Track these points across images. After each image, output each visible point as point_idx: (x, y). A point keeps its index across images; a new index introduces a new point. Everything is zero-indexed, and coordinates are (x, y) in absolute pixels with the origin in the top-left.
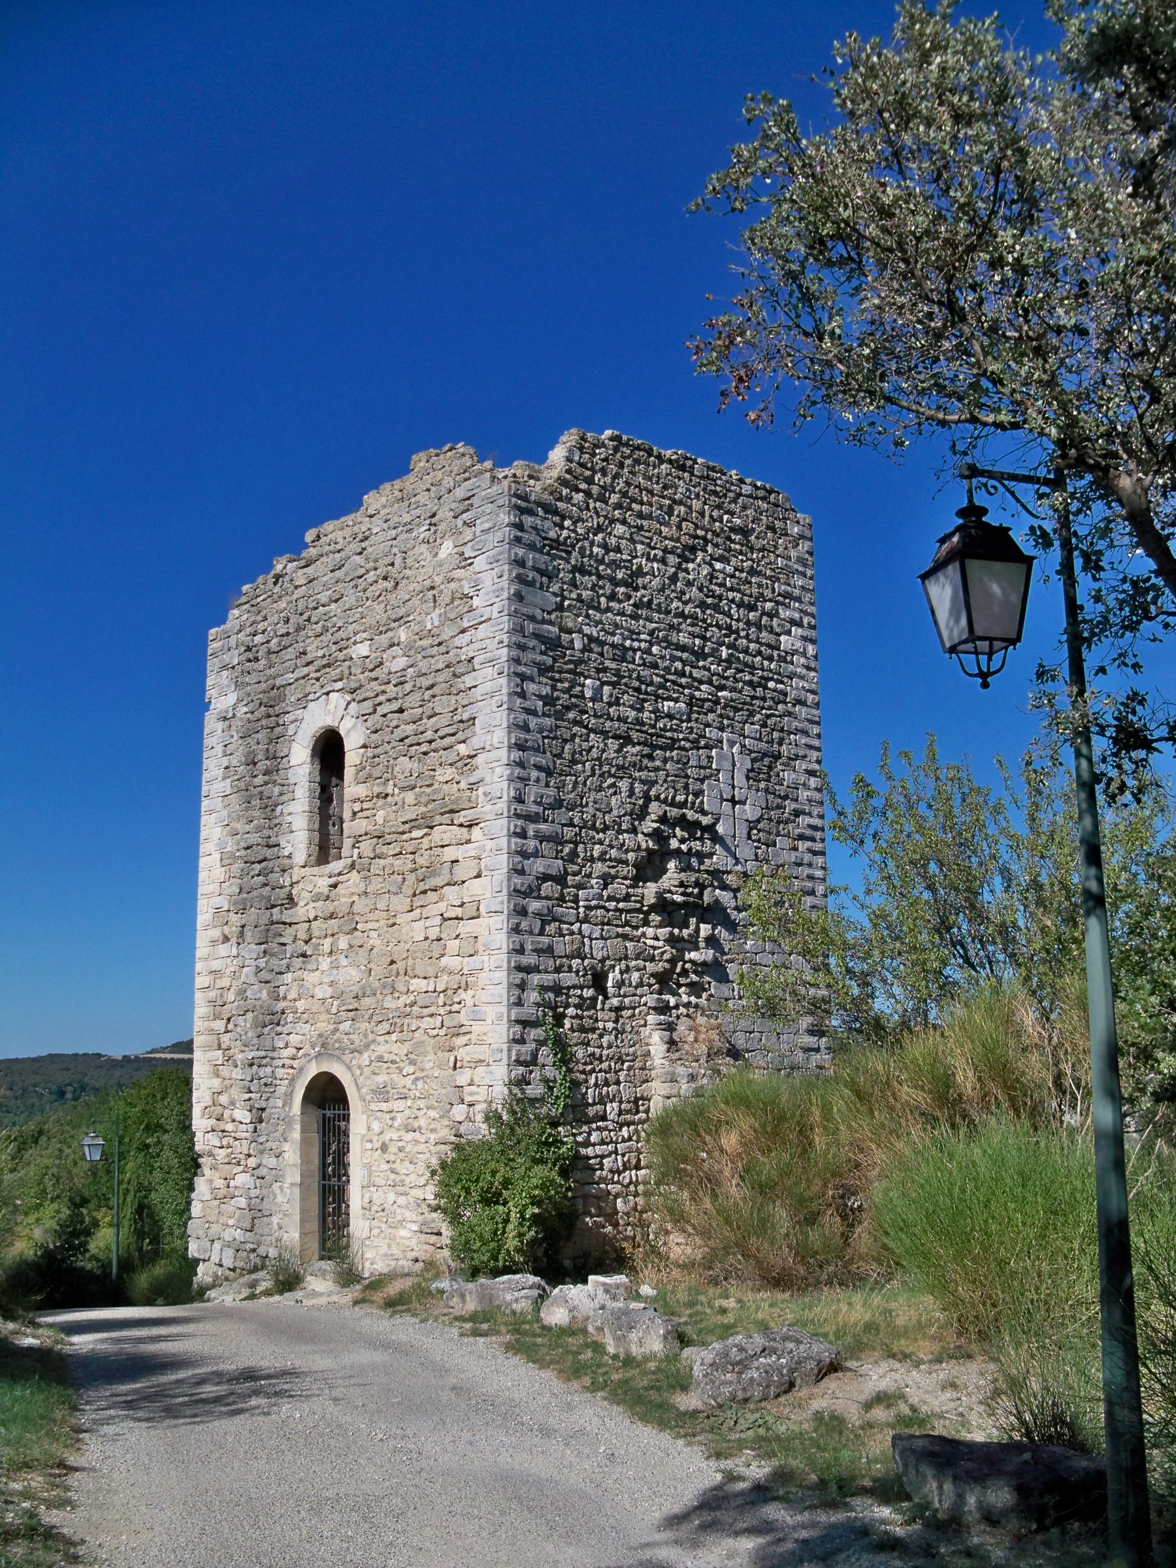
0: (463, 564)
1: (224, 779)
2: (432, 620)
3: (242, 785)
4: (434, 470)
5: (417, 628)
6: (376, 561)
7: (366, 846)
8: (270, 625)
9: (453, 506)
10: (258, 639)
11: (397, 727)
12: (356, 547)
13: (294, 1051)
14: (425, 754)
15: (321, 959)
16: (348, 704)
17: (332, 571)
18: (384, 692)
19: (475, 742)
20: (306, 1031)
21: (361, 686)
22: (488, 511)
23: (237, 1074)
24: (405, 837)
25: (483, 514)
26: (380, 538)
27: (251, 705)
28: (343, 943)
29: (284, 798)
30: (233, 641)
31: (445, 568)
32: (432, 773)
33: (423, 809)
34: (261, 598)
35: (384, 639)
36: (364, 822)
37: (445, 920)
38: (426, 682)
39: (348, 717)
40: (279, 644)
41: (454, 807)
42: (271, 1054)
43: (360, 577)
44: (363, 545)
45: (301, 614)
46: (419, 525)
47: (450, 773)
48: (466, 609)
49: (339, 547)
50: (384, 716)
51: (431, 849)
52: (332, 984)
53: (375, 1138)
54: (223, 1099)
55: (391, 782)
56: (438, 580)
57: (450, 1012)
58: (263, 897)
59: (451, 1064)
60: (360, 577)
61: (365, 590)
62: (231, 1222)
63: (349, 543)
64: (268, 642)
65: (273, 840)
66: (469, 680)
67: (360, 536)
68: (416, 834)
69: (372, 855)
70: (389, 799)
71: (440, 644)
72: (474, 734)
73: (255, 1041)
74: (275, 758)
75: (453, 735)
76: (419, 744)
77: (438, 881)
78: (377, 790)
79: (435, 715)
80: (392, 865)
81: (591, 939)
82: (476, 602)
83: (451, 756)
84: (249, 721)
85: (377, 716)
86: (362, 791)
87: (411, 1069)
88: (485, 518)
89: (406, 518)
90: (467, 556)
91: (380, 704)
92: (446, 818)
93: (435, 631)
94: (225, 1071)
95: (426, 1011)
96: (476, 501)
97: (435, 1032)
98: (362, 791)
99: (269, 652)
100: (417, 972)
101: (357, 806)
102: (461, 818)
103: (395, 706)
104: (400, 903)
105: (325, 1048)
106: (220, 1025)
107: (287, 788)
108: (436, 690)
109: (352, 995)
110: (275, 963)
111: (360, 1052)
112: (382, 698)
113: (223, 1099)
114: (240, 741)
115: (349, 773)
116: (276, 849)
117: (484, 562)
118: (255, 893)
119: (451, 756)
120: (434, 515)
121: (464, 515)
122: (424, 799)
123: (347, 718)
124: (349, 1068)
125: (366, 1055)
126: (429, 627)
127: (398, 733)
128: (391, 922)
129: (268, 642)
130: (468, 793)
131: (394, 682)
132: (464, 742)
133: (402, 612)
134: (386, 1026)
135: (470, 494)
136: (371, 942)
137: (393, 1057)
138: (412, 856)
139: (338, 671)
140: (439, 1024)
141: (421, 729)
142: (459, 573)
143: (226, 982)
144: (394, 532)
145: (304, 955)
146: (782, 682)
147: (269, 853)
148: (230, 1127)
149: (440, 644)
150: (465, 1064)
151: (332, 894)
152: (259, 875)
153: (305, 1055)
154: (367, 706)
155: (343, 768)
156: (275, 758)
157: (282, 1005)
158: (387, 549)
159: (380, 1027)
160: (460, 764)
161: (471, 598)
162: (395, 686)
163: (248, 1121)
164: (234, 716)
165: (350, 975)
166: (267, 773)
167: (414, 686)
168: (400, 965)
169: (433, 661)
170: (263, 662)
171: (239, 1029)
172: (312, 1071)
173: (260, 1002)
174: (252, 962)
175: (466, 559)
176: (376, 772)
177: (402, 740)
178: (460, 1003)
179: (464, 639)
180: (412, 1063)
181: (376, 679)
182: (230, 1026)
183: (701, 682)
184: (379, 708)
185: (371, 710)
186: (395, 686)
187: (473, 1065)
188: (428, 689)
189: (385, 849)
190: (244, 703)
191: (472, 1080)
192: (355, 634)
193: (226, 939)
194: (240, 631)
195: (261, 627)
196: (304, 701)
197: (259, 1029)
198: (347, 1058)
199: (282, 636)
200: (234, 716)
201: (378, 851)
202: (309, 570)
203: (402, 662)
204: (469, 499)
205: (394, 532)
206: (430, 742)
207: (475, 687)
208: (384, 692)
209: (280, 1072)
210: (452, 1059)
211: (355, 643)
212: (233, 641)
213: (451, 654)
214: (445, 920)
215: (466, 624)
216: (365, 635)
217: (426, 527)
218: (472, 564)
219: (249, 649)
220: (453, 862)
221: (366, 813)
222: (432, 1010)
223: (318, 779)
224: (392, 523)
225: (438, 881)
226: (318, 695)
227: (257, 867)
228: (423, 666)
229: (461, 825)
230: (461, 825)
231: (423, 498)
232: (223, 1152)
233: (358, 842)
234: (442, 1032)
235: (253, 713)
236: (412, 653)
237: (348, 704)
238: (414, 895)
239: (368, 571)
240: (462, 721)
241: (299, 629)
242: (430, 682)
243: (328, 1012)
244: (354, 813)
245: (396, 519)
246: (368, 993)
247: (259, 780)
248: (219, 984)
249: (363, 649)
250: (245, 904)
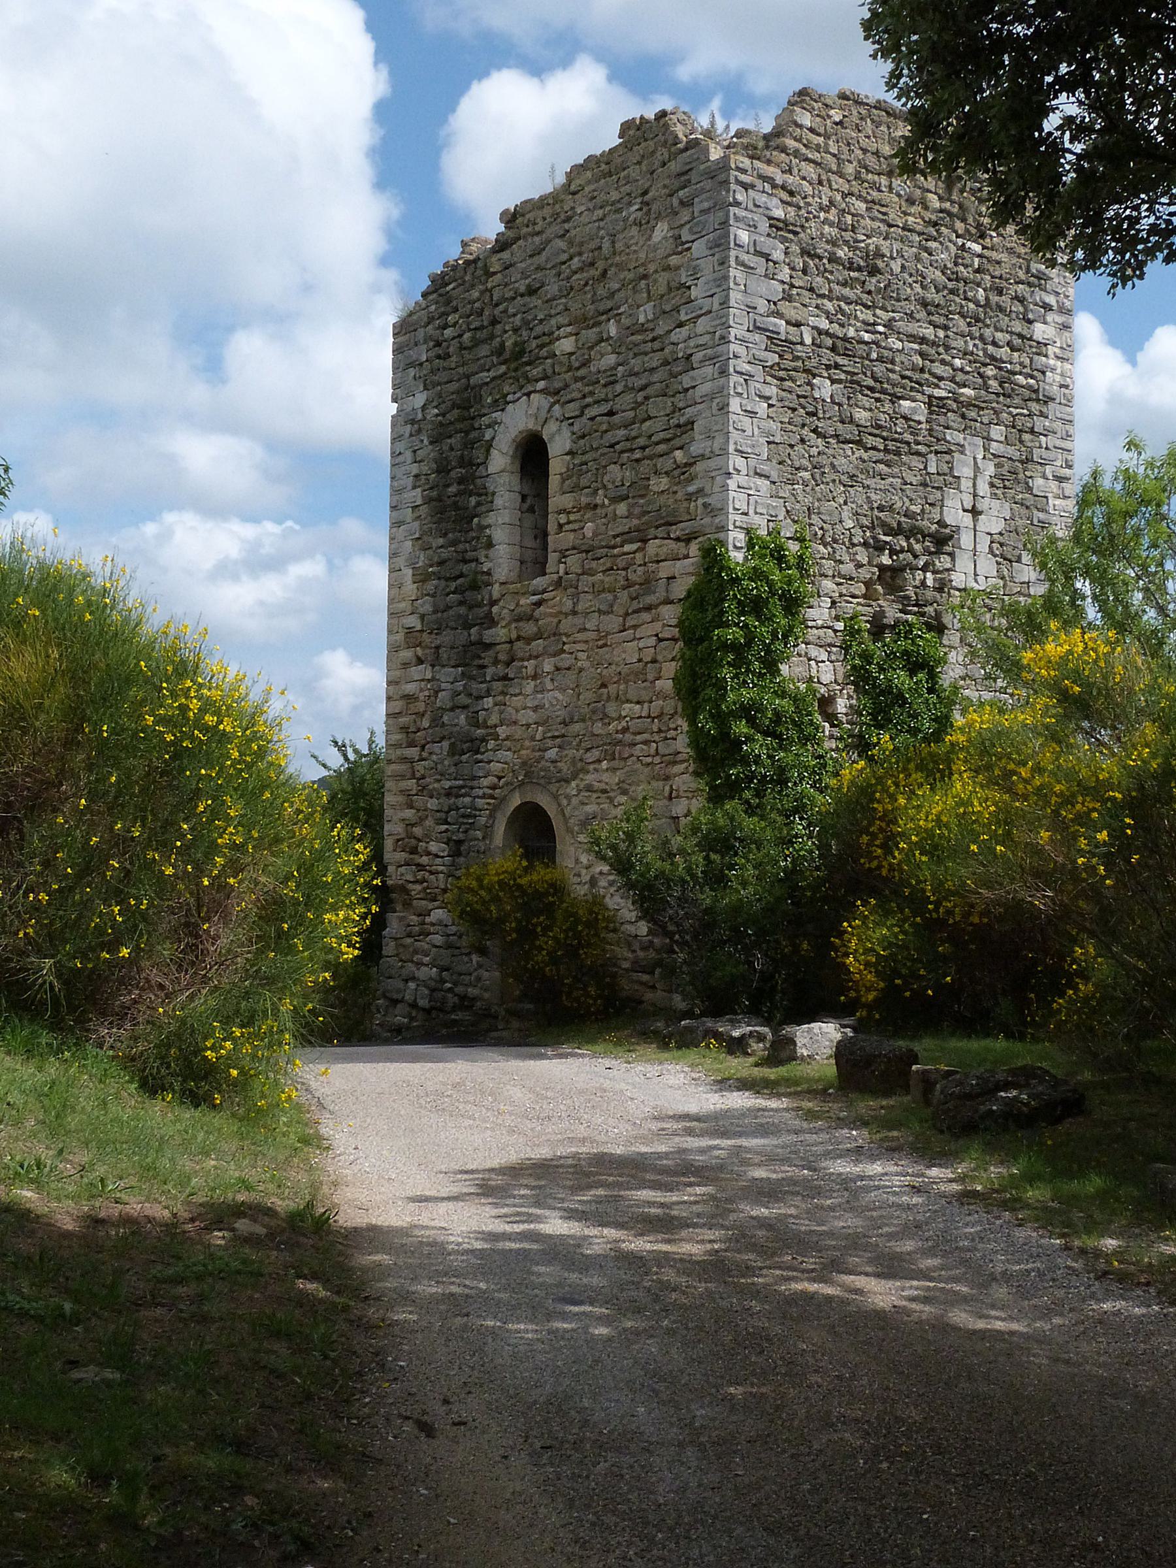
0: (680, 249)
1: (414, 487)
2: (644, 314)
3: (435, 494)
4: (646, 140)
5: (625, 321)
6: (581, 244)
7: (573, 561)
8: (460, 317)
9: (667, 182)
10: (448, 332)
11: (606, 431)
12: (556, 229)
13: (496, 780)
14: (637, 461)
15: (524, 682)
16: (551, 406)
17: (530, 256)
18: (592, 393)
19: (695, 449)
20: (508, 760)
21: (567, 386)
22: (708, 188)
23: (432, 804)
24: (616, 551)
25: (703, 190)
26: (585, 219)
27: (443, 406)
28: (548, 666)
29: (483, 509)
30: (421, 333)
31: (661, 253)
32: (645, 483)
33: (635, 522)
34: (451, 286)
35: (591, 334)
36: (572, 536)
37: (660, 640)
38: (639, 382)
39: (553, 420)
40: (473, 338)
41: (670, 519)
42: (469, 783)
43: (564, 263)
44: (566, 226)
45: (497, 305)
46: (630, 204)
47: (664, 482)
48: (683, 301)
49: (537, 228)
50: (592, 419)
51: (645, 564)
52: (535, 709)
53: (584, 871)
54: (417, 831)
55: (600, 492)
56: (652, 268)
57: (666, 739)
58: (460, 616)
59: (667, 794)
60: (564, 263)
61: (569, 278)
62: (426, 960)
63: (550, 224)
64: (460, 336)
65: (470, 555)
66: (686, 381)
67: (563, 216)
68: (628, 548)
69: (580, 571)
70: (598, 511)
71: (654, 340)
72: (693, 440)
73: (453, 769)
74: (471, 464)
75: (669, 440)
76: (632, 450)
77: (649, 599)
78: (584, 500)
79: (650, 418)
80: (602, 581)
81: (817, 662)
82: (694, 292)
83: (667, 464)
84: (441, 424)
85: (584, 419)
86: (567, 501)
87: (623, 799)
88: (704, 196)
89: (615, 196)
90: (684, 239)
91: (588, 406)
92: (661, 532)
93: (651, 325)
94: (419, 801)
95: (639, 738)
96: (694, 175)
97: (649, 760)
98: (567, 501)
99: (462, 348)
100: (629, 696)
101: (563, 519)
102: (676, 531)
103: (604, 408)
104: (612, 622)
105: (530, 775)
106: (413, 752)
107: (486, 496)
108: (650, 391)
109: (559, 720)
110: (475, 687)
111: (567, 781)
112: (589, 400)
113: (417, 831)
114: (430, 447)
115: (554, 481)
116: (473, 565)
117: (704, 247)
118: (451, 612)
119: (667, 464)
120: (645, 193)
121: (681, 193)
122: (637, 511)
123: (1008, 336)
124: (556, 797)
125: (573, 784)
126: (642, 319)
127: (609, 438)
128: (600, 643)
129: (460, 336)
130: (685, 504)
131: (602, 382)
132: (681, 448)
133: (609, 304)
134: (596, 753)
135: (688, 167)
136: (579, 664)
137: (603, 786)
138: (624, 573)
139: (540, 369)
140: (653, 751)
141: (633, 434)
142: (674, 260)
143: (421, 706)
144: (600, 212)
145: (505, 678)
146: (1032, 377)
147: (465, 568)
148: (425, 860)
149: (654, 340)
150: (681, 793)
151: (537, 613)
152: (454, 593)
153: (507, 784)
154: (572, 409)
155: (548, 476)
156: (471, 464)
157: (480, 732)
158: (594, 231)
159: (589, 754)
160: (676, 473)
161: (689, 288)
162: (605, 386)
163: (446, 854)
164: (424, 419)
165: (555, 698)
166: (461, 481)
167: (626, 386)
168: (612, 689)
169: (646, 359)
170: (454, 359)
171: (434, 757)
172: (516, 801)
173: (458, 728)
174: (449, 686)
175: (683, 243)
176: (584, 482)
177: (612, 446)
178: (676, 729)
179: (684, 332)
180: (624, 792)
181: (583, 378)
182: (425, 754)
183: (941, 379)
184: (586, 412)
185: (577, 413)
186: (605, 386)
187: (690, 795)
188: (641, 390)
189: (594, 564)
190: (435, 404)
191: (689, 811)
192: (559, 328)
193: (420, 661)
194: (429, 323)
195: (451, 319)
196: (501, 404)
197: (457, 757)
198: (553, 788)
199: (475, 329)
200: (424, 419)
201: (587, 567)
202: (505, 255)
203: (611, 359)
204: (687, 172)
205: (600, 212)
206: (643, 448)
207: (694, 387)
208: (592, 393)
209: (480, 803)
210: (667, 788)
211: (558, 339)
212: (421, 333)
213: (666, 351)
214: (660, 640)
215: (683, 317)
216: (569, 329)
217: (637, 207)
218: (689, 249)
219: (438, 344)
220: (668, 578)
221: (571, 527)
222: (646, 736)
223: (517, 488)
224: (598, 201)
225: (649, 599)
226: (517, 395)
227: (453, 585)
228: (636, 363)
229: (678, 539)
230: (678, 539)
231: (633, 172)
232: (418, 887)
233: (565, 557)
234: (657, 760)
235: (443, 415)
236: (623, 349)
237: (551, 406)
238: (627, 614)
239: (571, 258)
240: (679, 426)
241: (494, 322)
242: (643, 382)
243: (533, 739)
244: (561, 526)
245: (603, 197)
246: (576, 718)
247: (453, 489)
248: (413, 708)
249: (566, 345)
250: (441, 624)
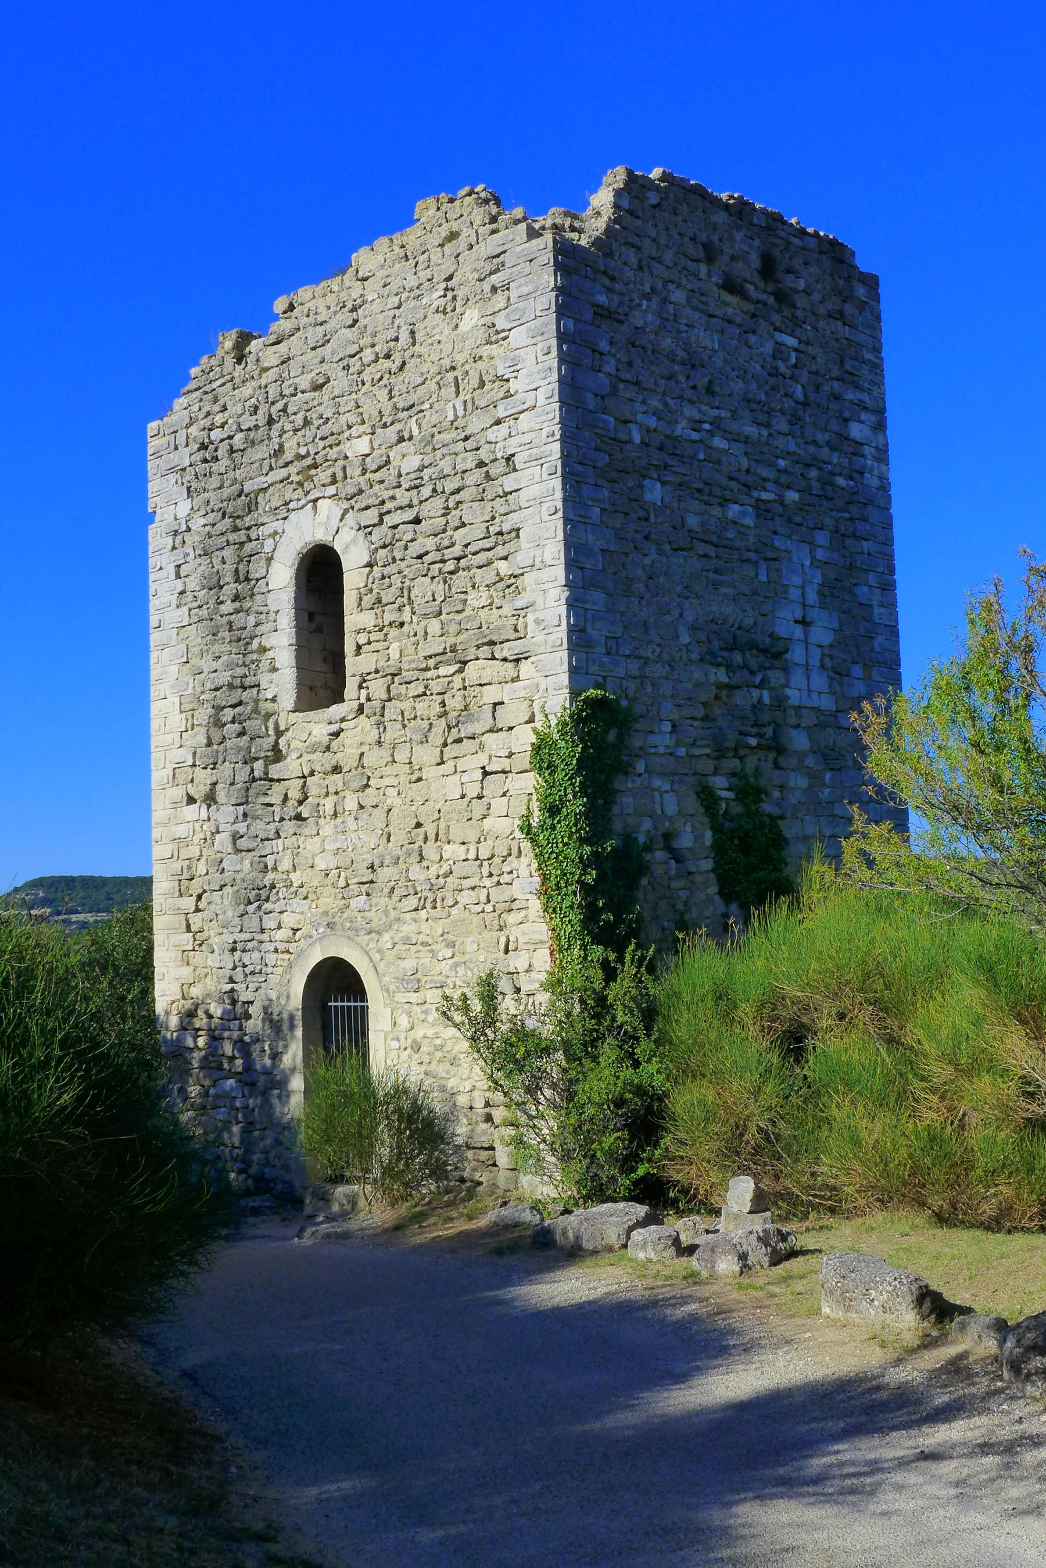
3: (204, 613)
11: (412, 540)
12: (347, 318)
16: (345, 512)
17: (313, 349)
19: (522, 558)
24: (429, 674)
31: (469, 344)
32: (463, 596)
34: (218, 383)
35: (391, 433)
38: (451, 485)
41: (494, 638)
43: (353, 356)
45: (273, 403)
48: (501, 395)
49: (320, 319)
50: (395, 527)
56: (460, 358)
60: (353, 356)
63: (335, 313)
64: (231, 437)
65: (248, 681)
66: (509, 483)
67: (349, 306)
68: (443, 671)
71: (466, 439)
75: (489, 550)
79: (464, 525)
82: (513, 386)
83: (488, 574)
90: (499, 328)
91: (389, 512)
92: (485, 651)
98: (367, 619)
103: (409, 515)
104: (427, 755)
107: (263, 615)
116: (255, 690)
120: (450, 278)
121: (494, 277)
127: (415, 549)
130: (513, 620)
131: (405, 486)
132: (505, 558)
138: (439, 698)
142: (485, 350)
149: (466, 439)
154: (371, 517)
161: (508, 380)
175: (497, 332)
184: (386, 518)
186: (408, 490)
188: (453, 493)
202: (282, 348)
204: (498, 256)
206: (458, 559)
208: (393, 498)
215: (501, 413)
217: (442, 293)
220: (495, 705)
224: (394, 287)
226: (303, 502)
229: (505, 660)
230: (505, 660)
233: (365, 681)
237: (345, 512)
242: (456, 485)
244: (359, 647)
249: (362, 446)
